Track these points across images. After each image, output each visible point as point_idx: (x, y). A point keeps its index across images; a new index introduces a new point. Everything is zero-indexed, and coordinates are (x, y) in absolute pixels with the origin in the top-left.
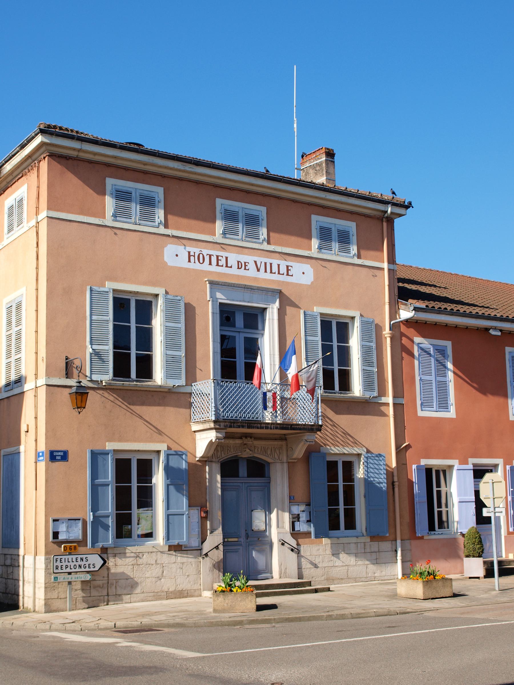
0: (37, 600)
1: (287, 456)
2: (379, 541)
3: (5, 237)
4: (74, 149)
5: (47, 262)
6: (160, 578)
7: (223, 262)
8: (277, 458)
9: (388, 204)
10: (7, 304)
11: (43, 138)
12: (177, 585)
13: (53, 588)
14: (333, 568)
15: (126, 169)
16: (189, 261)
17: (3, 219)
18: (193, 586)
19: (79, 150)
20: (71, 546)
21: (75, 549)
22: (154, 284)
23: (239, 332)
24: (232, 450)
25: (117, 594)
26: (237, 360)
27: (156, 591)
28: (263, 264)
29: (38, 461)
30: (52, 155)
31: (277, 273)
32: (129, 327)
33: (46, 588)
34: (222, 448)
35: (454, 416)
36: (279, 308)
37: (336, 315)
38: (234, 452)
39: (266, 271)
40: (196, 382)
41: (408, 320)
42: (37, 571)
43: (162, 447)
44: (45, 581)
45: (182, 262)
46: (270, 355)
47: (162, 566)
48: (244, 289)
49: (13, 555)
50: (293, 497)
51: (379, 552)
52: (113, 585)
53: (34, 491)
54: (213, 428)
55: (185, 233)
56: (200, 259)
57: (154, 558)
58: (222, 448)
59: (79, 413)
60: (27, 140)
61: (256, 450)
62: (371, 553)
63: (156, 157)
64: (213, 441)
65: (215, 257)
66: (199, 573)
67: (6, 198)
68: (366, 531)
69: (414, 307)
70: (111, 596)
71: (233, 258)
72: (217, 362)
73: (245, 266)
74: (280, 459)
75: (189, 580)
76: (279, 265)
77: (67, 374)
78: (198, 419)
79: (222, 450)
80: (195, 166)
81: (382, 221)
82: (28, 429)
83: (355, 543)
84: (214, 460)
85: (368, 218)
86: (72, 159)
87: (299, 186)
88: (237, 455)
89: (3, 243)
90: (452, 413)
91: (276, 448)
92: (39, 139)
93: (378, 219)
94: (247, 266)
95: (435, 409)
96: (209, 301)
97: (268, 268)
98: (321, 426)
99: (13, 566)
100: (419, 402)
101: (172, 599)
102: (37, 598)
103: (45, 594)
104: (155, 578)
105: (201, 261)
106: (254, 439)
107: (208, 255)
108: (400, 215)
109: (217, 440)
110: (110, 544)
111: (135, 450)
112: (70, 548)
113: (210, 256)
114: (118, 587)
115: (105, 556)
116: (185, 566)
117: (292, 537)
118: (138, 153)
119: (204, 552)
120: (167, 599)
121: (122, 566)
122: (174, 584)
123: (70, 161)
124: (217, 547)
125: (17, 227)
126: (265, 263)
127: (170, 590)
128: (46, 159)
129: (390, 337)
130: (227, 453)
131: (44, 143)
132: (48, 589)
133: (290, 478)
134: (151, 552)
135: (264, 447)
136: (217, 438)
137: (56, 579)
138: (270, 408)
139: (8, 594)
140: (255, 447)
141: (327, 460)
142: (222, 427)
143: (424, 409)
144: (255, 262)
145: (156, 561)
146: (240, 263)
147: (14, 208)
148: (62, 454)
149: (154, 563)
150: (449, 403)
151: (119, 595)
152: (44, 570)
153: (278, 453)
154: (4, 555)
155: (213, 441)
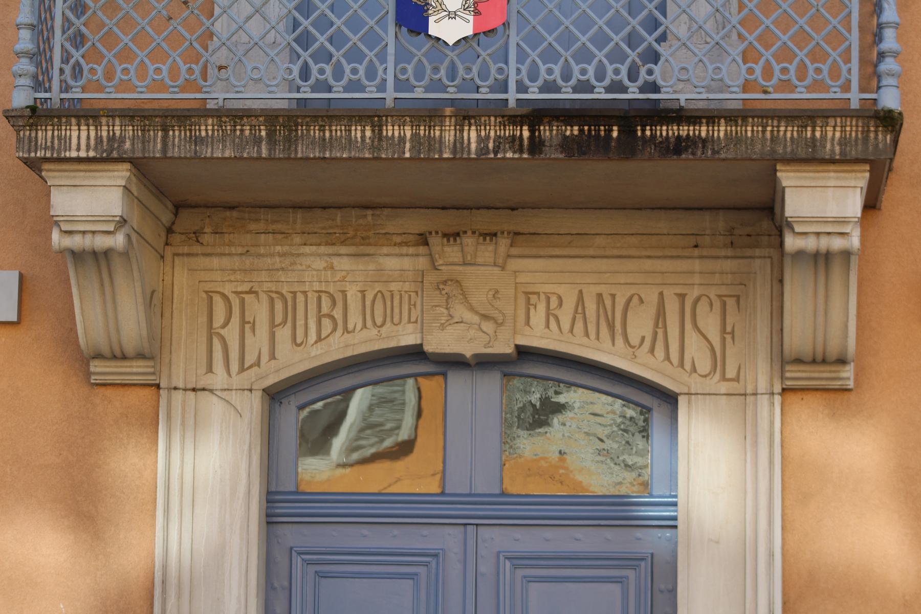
8: (704, 366)
24: (355, 319)
34: (279, 306)
58: (279, 306)
61: (538, 316)
74: (731, 373)
79: (279, 319)
91: (698, 299)
130: (313, 337)
138: (452, 15)
142: (83, 154)
153: (715, 338)
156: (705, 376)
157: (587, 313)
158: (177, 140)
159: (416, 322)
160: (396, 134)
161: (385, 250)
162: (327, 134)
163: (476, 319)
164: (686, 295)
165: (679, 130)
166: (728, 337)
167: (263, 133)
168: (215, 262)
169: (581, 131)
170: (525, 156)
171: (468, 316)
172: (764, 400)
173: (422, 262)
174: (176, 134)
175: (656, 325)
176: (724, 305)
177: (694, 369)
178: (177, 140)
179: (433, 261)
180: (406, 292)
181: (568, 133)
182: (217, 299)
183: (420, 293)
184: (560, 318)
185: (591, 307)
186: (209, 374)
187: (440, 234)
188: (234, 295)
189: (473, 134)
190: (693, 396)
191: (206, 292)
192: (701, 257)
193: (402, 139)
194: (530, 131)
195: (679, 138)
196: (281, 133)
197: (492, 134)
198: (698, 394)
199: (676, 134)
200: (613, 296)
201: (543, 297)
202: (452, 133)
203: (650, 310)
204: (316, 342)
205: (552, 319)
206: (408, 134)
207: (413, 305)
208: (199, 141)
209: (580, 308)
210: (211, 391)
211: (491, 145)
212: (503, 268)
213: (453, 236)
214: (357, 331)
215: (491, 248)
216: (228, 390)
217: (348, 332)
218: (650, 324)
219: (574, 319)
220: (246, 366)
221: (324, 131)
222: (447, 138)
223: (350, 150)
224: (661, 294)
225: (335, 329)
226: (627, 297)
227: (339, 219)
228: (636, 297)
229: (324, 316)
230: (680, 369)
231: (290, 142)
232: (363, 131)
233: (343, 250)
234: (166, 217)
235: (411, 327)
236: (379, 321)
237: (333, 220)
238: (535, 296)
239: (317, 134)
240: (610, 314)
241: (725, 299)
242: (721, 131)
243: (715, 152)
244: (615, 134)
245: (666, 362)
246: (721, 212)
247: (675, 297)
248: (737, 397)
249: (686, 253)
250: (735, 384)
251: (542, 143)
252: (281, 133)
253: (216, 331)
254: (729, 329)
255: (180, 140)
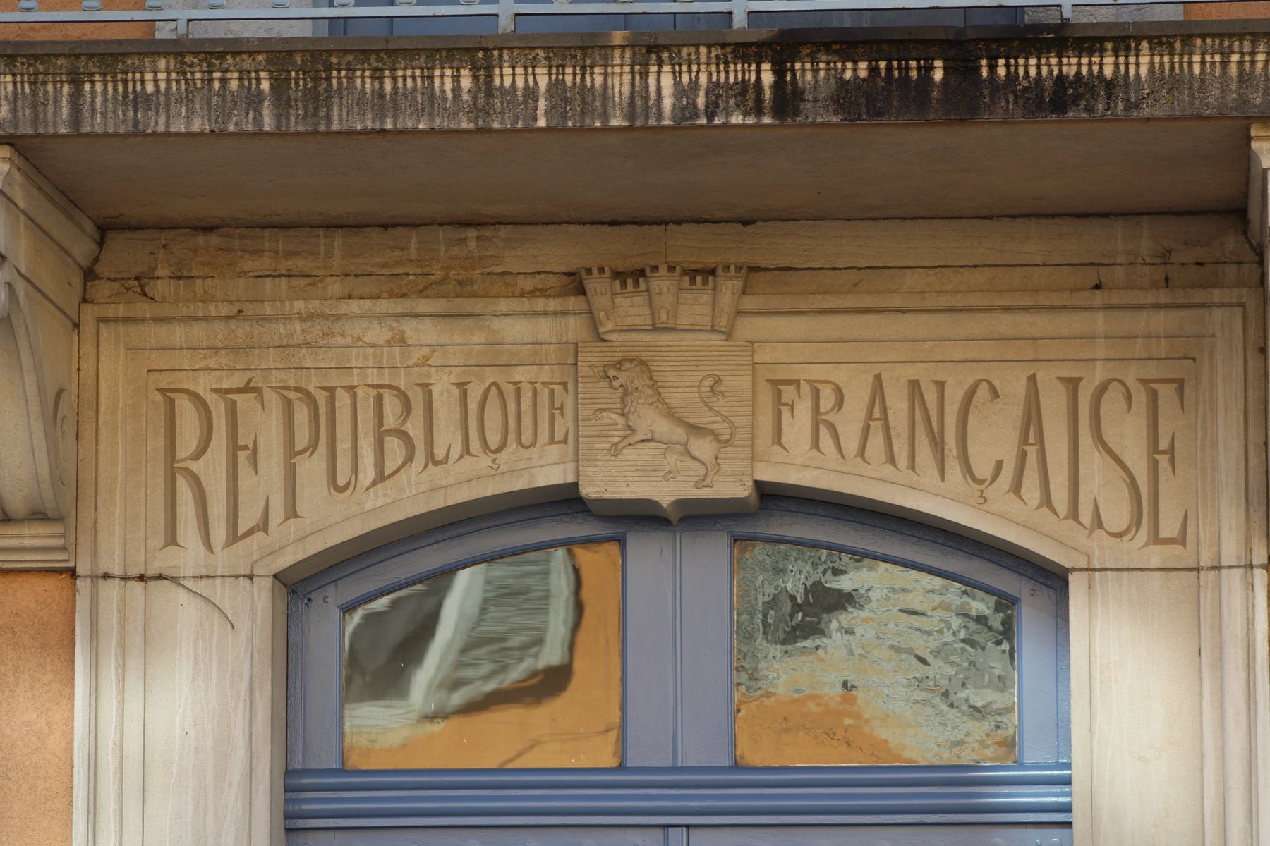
8: (1117, 514)
24: (447, 437)
34: (302, 415)
58: (302, 415)
61: (798, 426)
74: (1169, 528)
79: (302, 440)
135: (915, 385)
156: (1120, 535)
157: (891, 419)
158: (99, 101)
159: (565, 441)
160: (520, 82)
161: (503, 305)
162: (388, 85)
163: (679, 433)
164: (1080, 379)
165: (1060, 64)
166: (1163, 460)
167: (265, 85)
168: (178, 333)
169: (873, 70)
170: (767, 120)
171: (663, 427)
172: (1233, 579)
173: (574, 327)
174: (97, 90)
175: (1024, 440)
176: (1153, 399)
177: (1098, 523)
178: (99, 101)
179: (594, 325)
180: (544, 384)
181: (848, 75)
182: (185, 408)
183: (570, 387)
184: (839, 429)
185: (898, 406)
186: (172, 547)
187: (607, 274)
188: (215, 396)
189: (667, 81)
190: (1097, 574)
191: (162, 391)
192: (1108, 307)
193: (531, 93)
194: (775, 72)
195: (1061, 78)
196: (299, 85)
197: (703, 79)
198: (1106, 569)
199: (1056, 72)
200: (941, 385)
201: (805, 389)
202: (627, 78)
203: (1012, 412)
204: (374, 483)
205: (823, 431)
206: (543, 82)
207: (556, 409)
208: (141, 101)
209: (877, 409)
210: (175, 580)
211: (701, 101)
212: (729, 335)
213: (632, 276)
214: (451, 460)
215: (705, 297)
216: (208, 577)
217: (436, 463)
218: (1013, 437)
219: (866, 430)
220: (241, 531)
221: (381, 79)
222: (617, 89)
223: (431, 115)
224: (1032, 379)
225: (409, 458)
226: (966, 387)
227: (413, 246)
228: (984, 385)
229: (390, 432)
230: (1071, 521)
231: (317, 101)
232: (456, 79)
233: (423, 306)
234: (82, 249)
235: (555, 450)
236: (494, 441)
237: (402, 249)
238: (791, 388)
239: (368, 86)
240: (934, 419)
241: (1155, 386)
242: (1143, 64)
243: (1130, 105)
244: (938, 75)
245: (1045, 510)
246: (1145, 218)
247: (1060, 387)
248: (1183, 573)
249: (1081, 299)
250: (1178, 549)
251: (798, 94)
252: (299, 85)
253: (183, 465)
254: (1164, 444)
255: (105, 100)
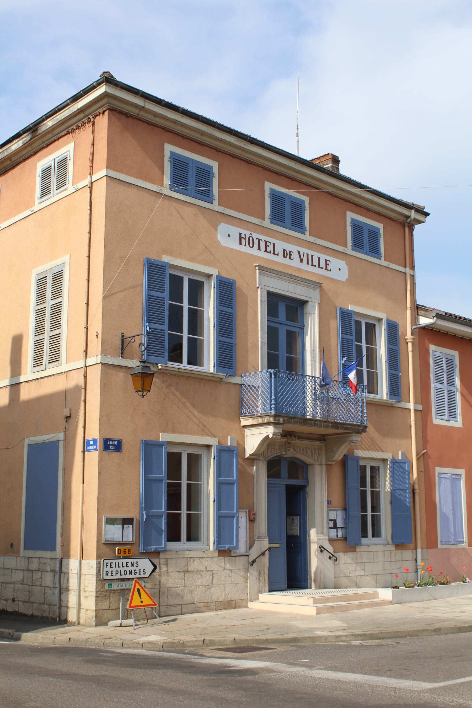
0: (83, 612)
1: (327, 459)
2: (402, 550)
3: (37, 202)
4: (136, 106)
5: (105, 226)
6: (210, 586)
7: (270, 249)
8: (317, 460)
9: (412, 209)
10: (37, 274)
11: (107, 88)
12: (226, 595)
13: (104, 597)
14: (364, 577)
15: (184, 137)
16: (240, 243)
17: (35, 182)
18: (240, 596)
19: (142, 108)
20: (125, 549)
21: (129, 552)
22: (208, 263)
23: (282, 324)
25: (168, 604)
26: (280, 353)
27: (206, 602)
28: (305, 255)
29: (87, 450)
30: (112, 110)
31: (317, 266)
32: (182, 308)
33: (97, 597)
35: (461, 426)
36: (319, 302)
37: (367, 315)
38: (279, 451)
39: (308, 263)
40: (247, 372)
41: (426, 327)
42: (83, 577)
43: (213, 441)
44: (96, 589)
45: (233, 244)
46: (311, 350)
47: (211, 573)
48: (289, 279)
49: (42, 558)
50: (330, 502)
51: (402, 561)
52: (165, 594)
53: (82, 485)
54: (272, 422)
55: (237, 213)
56: (250, 242)
57: (204, 564)
59: (143, 396)
60: (84, 91)
61: (298, 450)
62: (396, 562)
63: (214, 128)
64: (271, 436)
65: (264, 242)
66: (246, 581)
67: (39, 160)
68: (392, 539)
69: (437, 314)
70: (163, 607)
71: (280, 246)
72: (265, 354)
73: (290, 255)
74: (320, 461)
75: (237, 589)
76: (319, 258)
77: (122, 353)
78: (249, 413)
79: (268, 448)
80: (250, 143)
81: (404, 226)
82: (71, 415)
83: (383, 551)
84: (261, 458)
85: (392, 222)
86: (132, 117)
87: (339, 179)
88: (279, 455)
89: (33, 208)
90: (458, 423)
92: (102, 89)
93: (401, 223)
94: (292, 255)
95: (446, 417)
96: (258, 287)
97: (310, 261)
98: (366, 427)
99: (42, 572)
100: (434, 410)
101: (221, 610)
102: (83, 609)
103: (96, 605)
104: (205, 586)
105: (251, 245)
106: (297, 438)
107: (257, 240)
108: (420, 222)
109: (274, 436)
110: (162, 548)
111: (187, 443)
112: (124, 552)
113: (259, 240)
114: (169, 597)
115: (156, 561)
116: (233, 574)
117: (329, 544)
118: (199, 121)
119: (251, 558)
120: (216, 611)
121: (173, 573)
122: (222, 594)
123: (130, 120)
124: (263, 554)
125: (56, 190)
126: (308, 255)
127: (219, 600)
128: (107, 113)
129: (411, 342)
131: (106, 95)
132: (100, 598)
133: (328, 481)
134: (202, 558)
136: (274, 434)
137: (110, 586)
139: (32, 603)
140: (297, 446)
141: (360, 464)
143: (438, 417)
144: (299, 252)
145: (206, 568)
146: (285, 251)
147: (52, 170)
148: (116, 443)
149: (205, 570)
150: (457, 412)
151: (170, 605)
152: (95, 577)
153: (318, 455)
154: (27, 559)
155: (271, 436)
177: (316, 460)
